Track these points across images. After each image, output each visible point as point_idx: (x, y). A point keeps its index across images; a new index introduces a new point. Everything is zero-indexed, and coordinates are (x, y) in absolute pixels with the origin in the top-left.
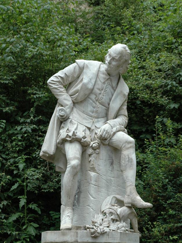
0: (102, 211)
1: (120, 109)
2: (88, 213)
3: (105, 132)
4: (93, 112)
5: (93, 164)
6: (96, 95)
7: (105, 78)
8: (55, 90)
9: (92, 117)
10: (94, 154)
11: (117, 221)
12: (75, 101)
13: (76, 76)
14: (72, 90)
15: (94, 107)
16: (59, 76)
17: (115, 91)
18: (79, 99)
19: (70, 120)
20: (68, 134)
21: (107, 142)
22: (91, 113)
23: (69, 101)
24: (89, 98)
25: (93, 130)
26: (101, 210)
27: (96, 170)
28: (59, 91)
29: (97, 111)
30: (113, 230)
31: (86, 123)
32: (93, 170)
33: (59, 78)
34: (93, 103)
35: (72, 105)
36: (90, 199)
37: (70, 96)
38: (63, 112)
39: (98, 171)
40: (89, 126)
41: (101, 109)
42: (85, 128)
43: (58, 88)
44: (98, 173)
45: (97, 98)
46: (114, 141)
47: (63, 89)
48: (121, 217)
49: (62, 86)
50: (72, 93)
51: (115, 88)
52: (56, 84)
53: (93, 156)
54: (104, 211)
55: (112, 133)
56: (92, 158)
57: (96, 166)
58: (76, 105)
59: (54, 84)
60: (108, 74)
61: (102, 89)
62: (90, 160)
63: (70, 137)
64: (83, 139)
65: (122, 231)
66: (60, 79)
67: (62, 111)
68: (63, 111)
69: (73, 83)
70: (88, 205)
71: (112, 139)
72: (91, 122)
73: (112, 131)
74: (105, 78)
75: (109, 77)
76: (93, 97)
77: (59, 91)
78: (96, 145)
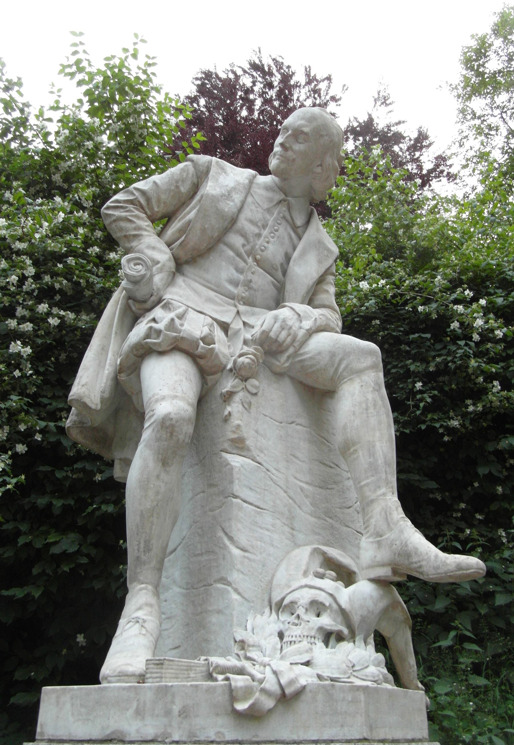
0: (276, 597)
3: (277, 325)
4: (235, 284)
5: (238, 426)
6: (244, 235)
7: (270, 200)
8: (123, 224)
9: (233, 299)
11: (340, 638)
12: (182, 255)
13: (184, 189)
16: (135, 189)
17: (300, 238)
20: (151, 328)
22: (231, 288)
23: (160, 251)
25: (237, 333)
27: (249, 450)
28: (133, 225)
29: (251, 281)
30: (332, 680)
31: (216, 311)
32: (237, 448)
33: (135, 192)
34: (238, 259)
36: (230, 552)
38: (139, 267)
39: (255, 453)
40: (226, 319)
42: (210, 320)
43: (130, 218)
44: (258, 459)
45: (248, 247)
46: (311, 358)
48: (356, 619)
50: (173, 234)
52: (127, 207)
53: (237, 398)
54: (283, 599)
55: (301, 333)
58: (188, 269)
59: (122, 207)
60: (278, 190)
62: (226, 413)
65: (369, 683)
67: (135, 265)
68: (138, 264)
70: (223, 580)
71: (302, 351)
73: (301, 328)
74: (270, 200)
75: (283, 196)
76: (236, 240)
77: (133, 225)
78: (247, 361)
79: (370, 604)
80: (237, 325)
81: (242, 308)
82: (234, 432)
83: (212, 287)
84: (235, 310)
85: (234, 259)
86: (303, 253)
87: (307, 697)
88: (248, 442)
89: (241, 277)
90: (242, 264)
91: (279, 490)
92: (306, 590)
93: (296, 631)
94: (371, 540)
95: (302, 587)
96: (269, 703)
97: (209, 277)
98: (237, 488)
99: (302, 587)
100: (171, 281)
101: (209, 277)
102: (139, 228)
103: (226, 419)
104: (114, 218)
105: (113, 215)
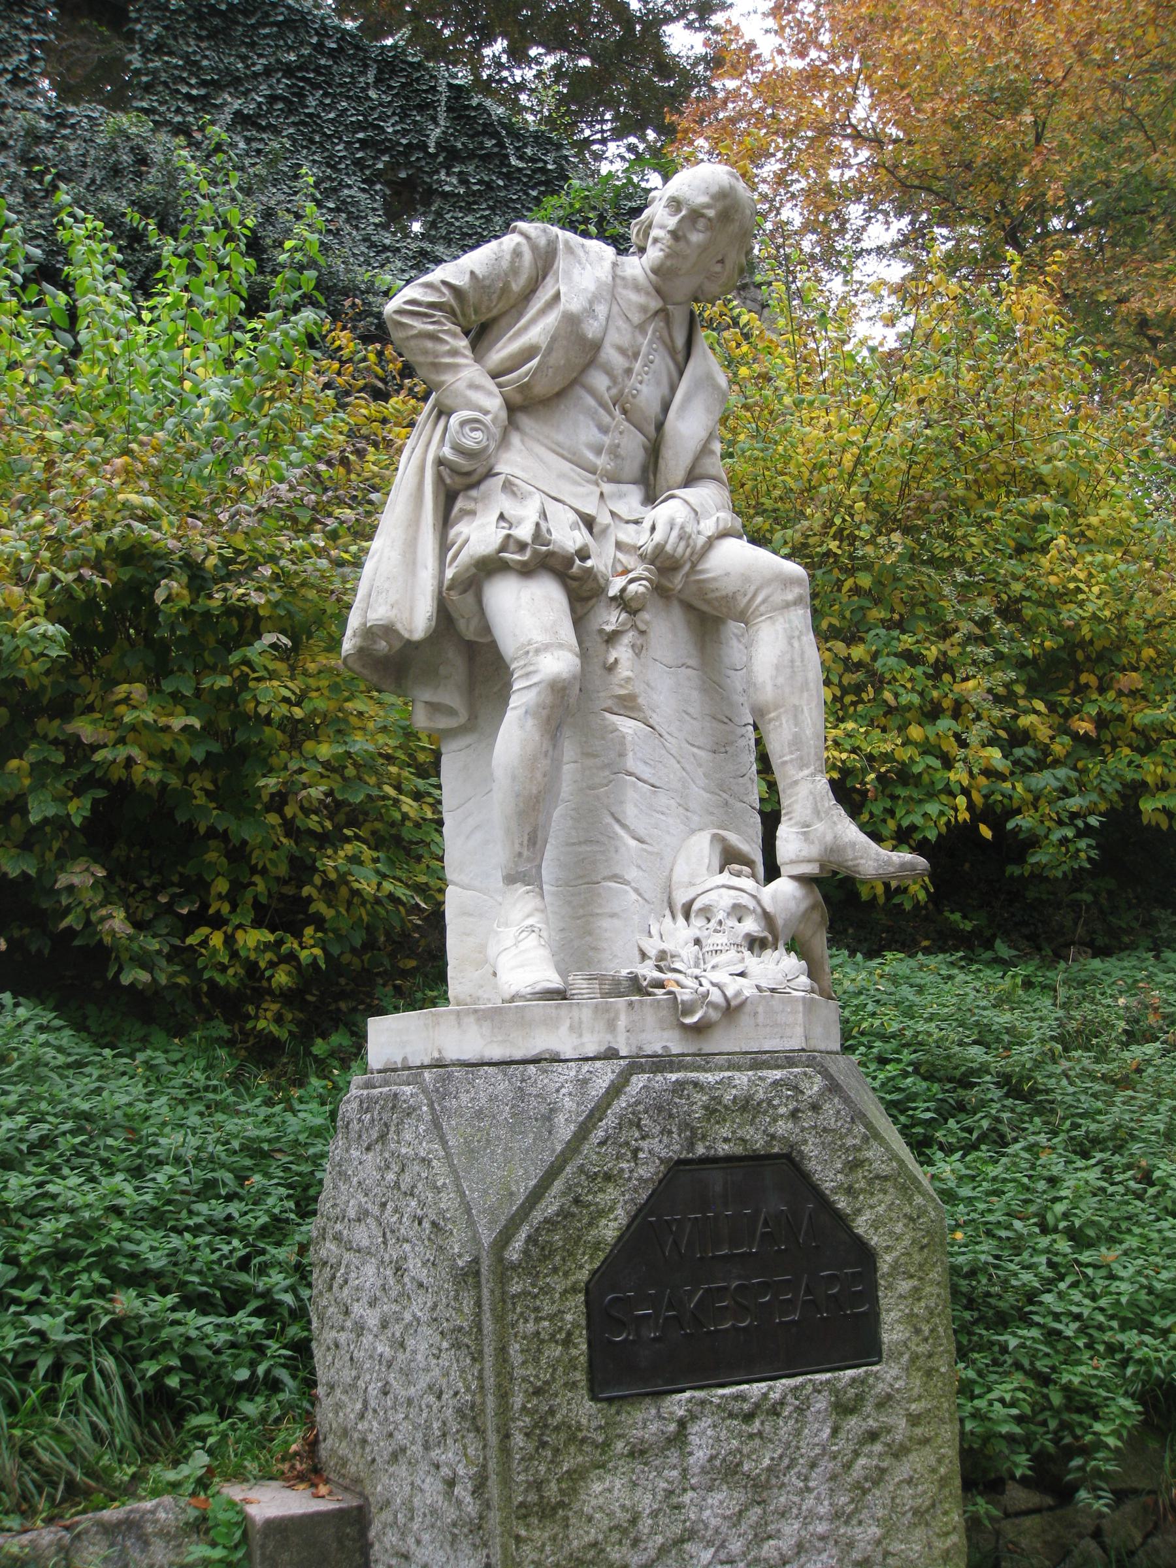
0: (681, 898)
1: (705, 450)
3: (675, 533)
4: (598, 451)
6: (609, 372)
7: (643, 309)
9: (594, 473)
10: (631, 634)
12: (517, 399)
13: (517, 286)
14: (502, 351)
15: (604, 430)
16: (444, 283)
18: (541, 388)
19: (496, 483)
20: (509, 536)
21: (678, 581)
22: (591, 456)
23: (490, 394)
24: (584, 387)
25: (605, 530)
27: (639, 709)
29: (618, 446)
30: (773, 990)
31: (575, 496)
32: (625, 707)
33: (444, 290)
34: (601, 411)
35: (504, 415)
36: (625, 844)
37: (494, 376)
40: (590, 510)
41: (633, 444)
42: (573, 517)
44: (652, 722)
45: (614, 391)
46: (714, 579)
47: (463, 343)
49: (458, 329)
50: (503, 361)
51: (680, 358)
52: (432, 316)
53: (627, 639)
54: (692, 902)
55: (701, 541)
56: (621, 652)
57: (638, 688)
58: (524, 420)
60: (654, 293)
61: (636, 355)
62: (611, 660)
63: (522, 546)
64: (578, 562)
66: (447, 297)
67: (473, 430)
68: (476, 429)
69: (503, 322)
70: (615, 878)
71: (699, 567)
72: (592, 493)
73: (699, 533)
74: (643, 309)
76: (600, 381)
77: (447, 348)
78: (642, 589)
79: (792, 905)
80: (604, 519)
81: (607, 488)
82: (621, 686)
83: (565, 453)
84: (597, 491)
85: (596, 412)
86: (688, 399)
87: (748, 1008)
88: (640, 700)
89: (607, 440)
90: (606, 419)
91: (673, 761)
92: (724, 890)
93: (721, 939)
94: (794, 830)
95: (718, 887)
96: (714, 1015)
97: (560, 437)
98: (631, 763)
99: (718, 887)
100: (504, 441)
101: (560, 437)
102: (454, 353)
103: (611, 668)
104: (415, 332)
105: (412, 327)
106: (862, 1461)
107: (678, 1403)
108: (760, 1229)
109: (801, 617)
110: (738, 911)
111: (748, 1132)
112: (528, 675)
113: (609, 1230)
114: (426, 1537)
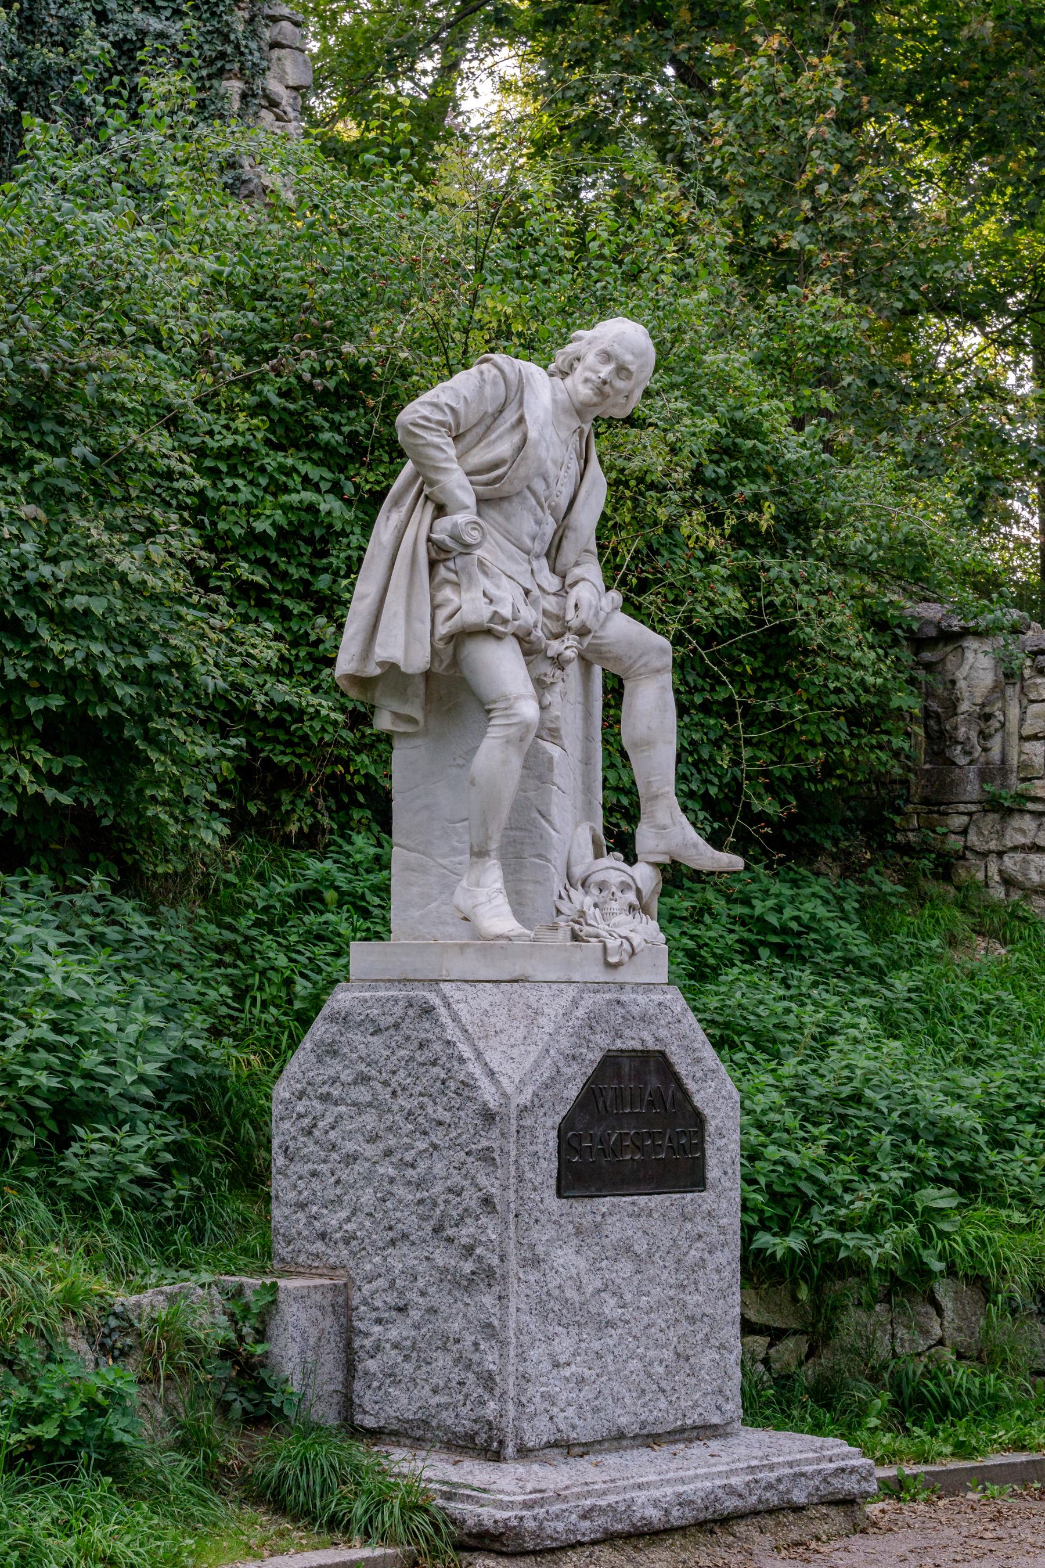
2: (537, 882)
5: (557, 718)
8: (433, 452)
26: (568, 868)
37: (468, 474)
63: (505, 621)
80: (536, 592)
93: (614, 905)
98: (557, 779)
106: (693, 1252)
107: (604, 1204)
108: (647, 1098)
109: (667, 679)
110: (624, 887)
111: (646, 1035)
112: (508, 716)
113: (573, 1092)
114: (431, 1290)
